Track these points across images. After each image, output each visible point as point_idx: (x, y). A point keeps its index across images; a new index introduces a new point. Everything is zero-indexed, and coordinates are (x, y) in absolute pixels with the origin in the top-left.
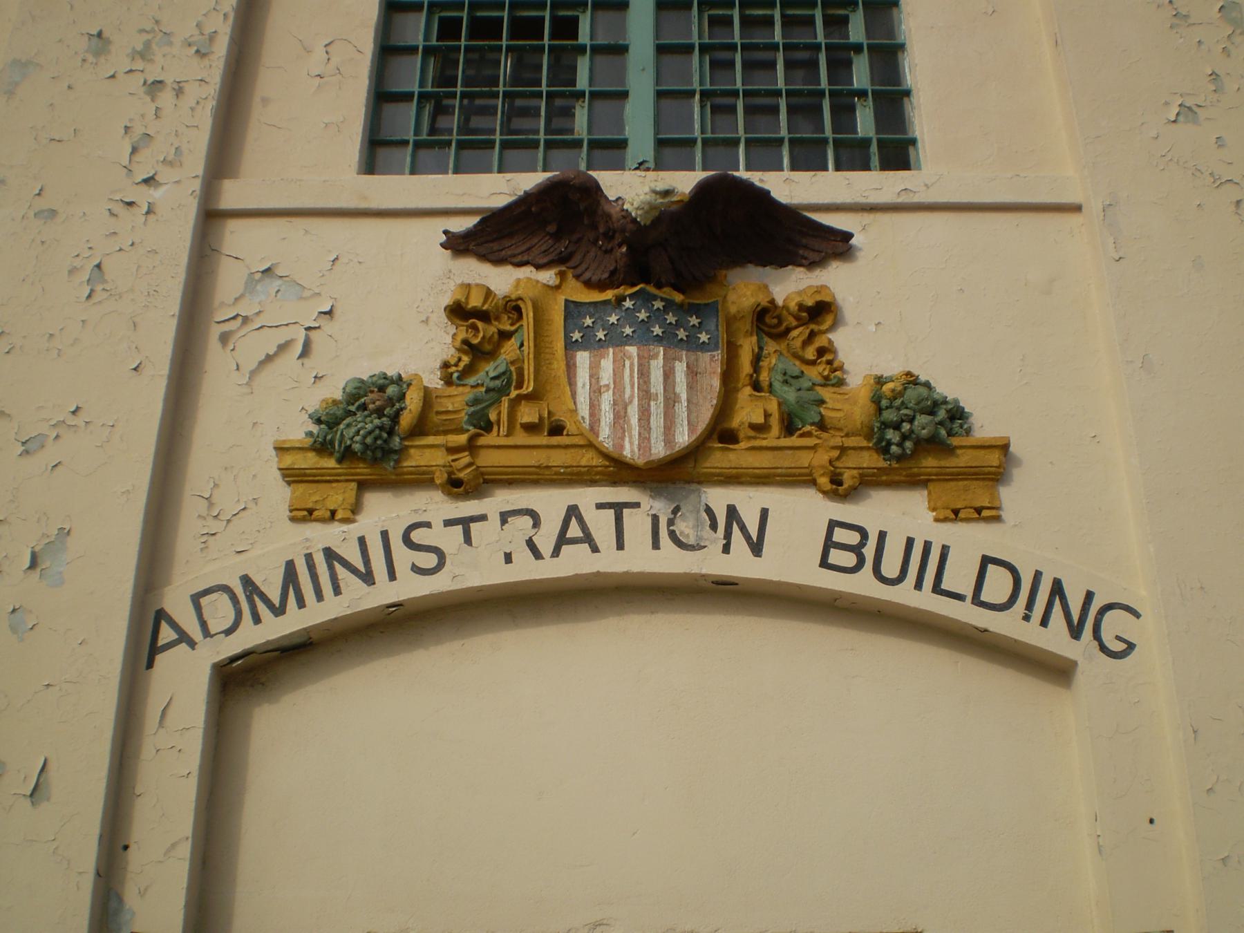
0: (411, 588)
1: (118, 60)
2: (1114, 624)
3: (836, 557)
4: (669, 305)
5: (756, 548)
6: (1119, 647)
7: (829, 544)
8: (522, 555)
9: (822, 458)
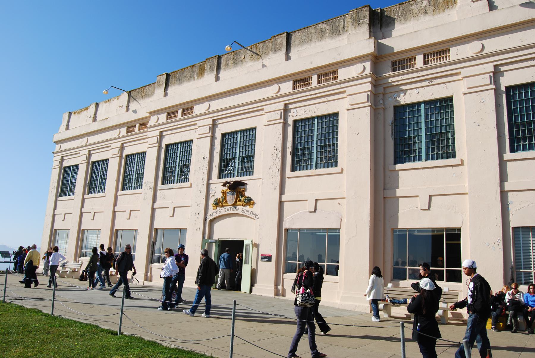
0: (219, 215)
1: (201, 170)
2: (258, 216)
3: (243, 211)
4: (232, 192)
5: (238, 211)
6: (258, 218)
7: (242, 210)
8: (225, 212)
9: (241, 204)
